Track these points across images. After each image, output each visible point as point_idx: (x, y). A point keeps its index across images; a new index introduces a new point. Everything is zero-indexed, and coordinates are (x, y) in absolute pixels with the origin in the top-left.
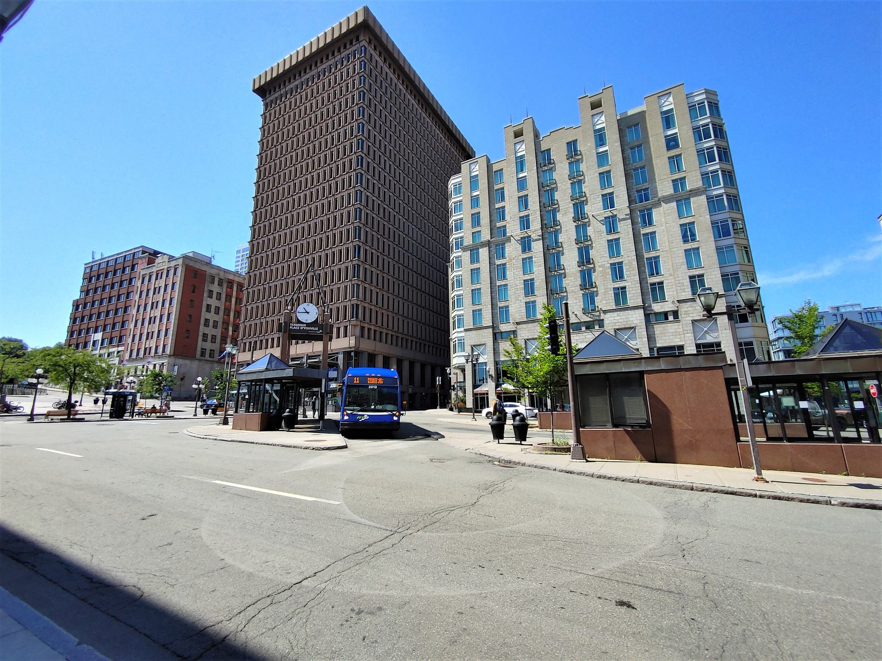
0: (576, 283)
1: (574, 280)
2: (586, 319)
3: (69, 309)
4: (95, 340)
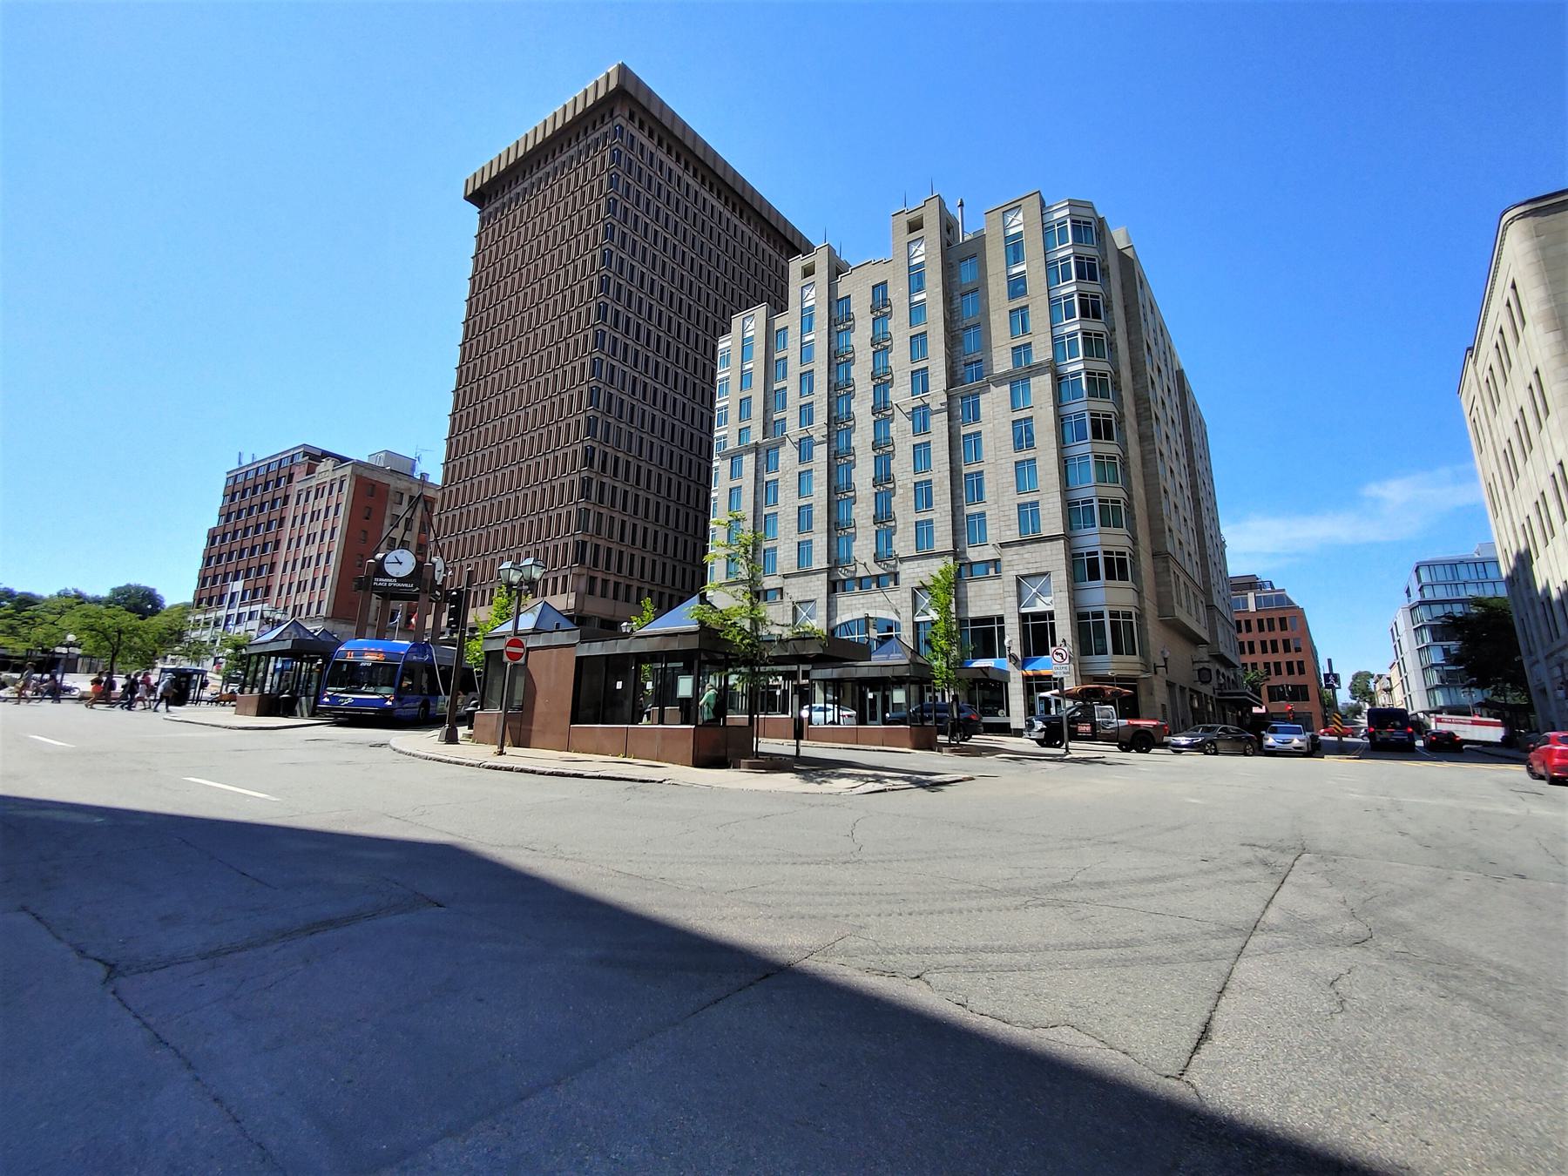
2: (877, 570)
3: (202, 543)
4: (234, 591)
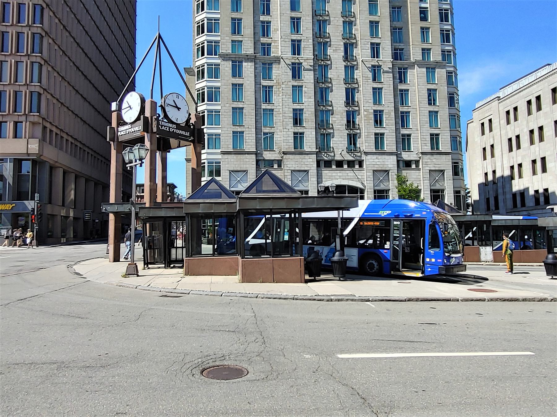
0: (342, 122)
1: (341, 119)
2: (349, 158)
